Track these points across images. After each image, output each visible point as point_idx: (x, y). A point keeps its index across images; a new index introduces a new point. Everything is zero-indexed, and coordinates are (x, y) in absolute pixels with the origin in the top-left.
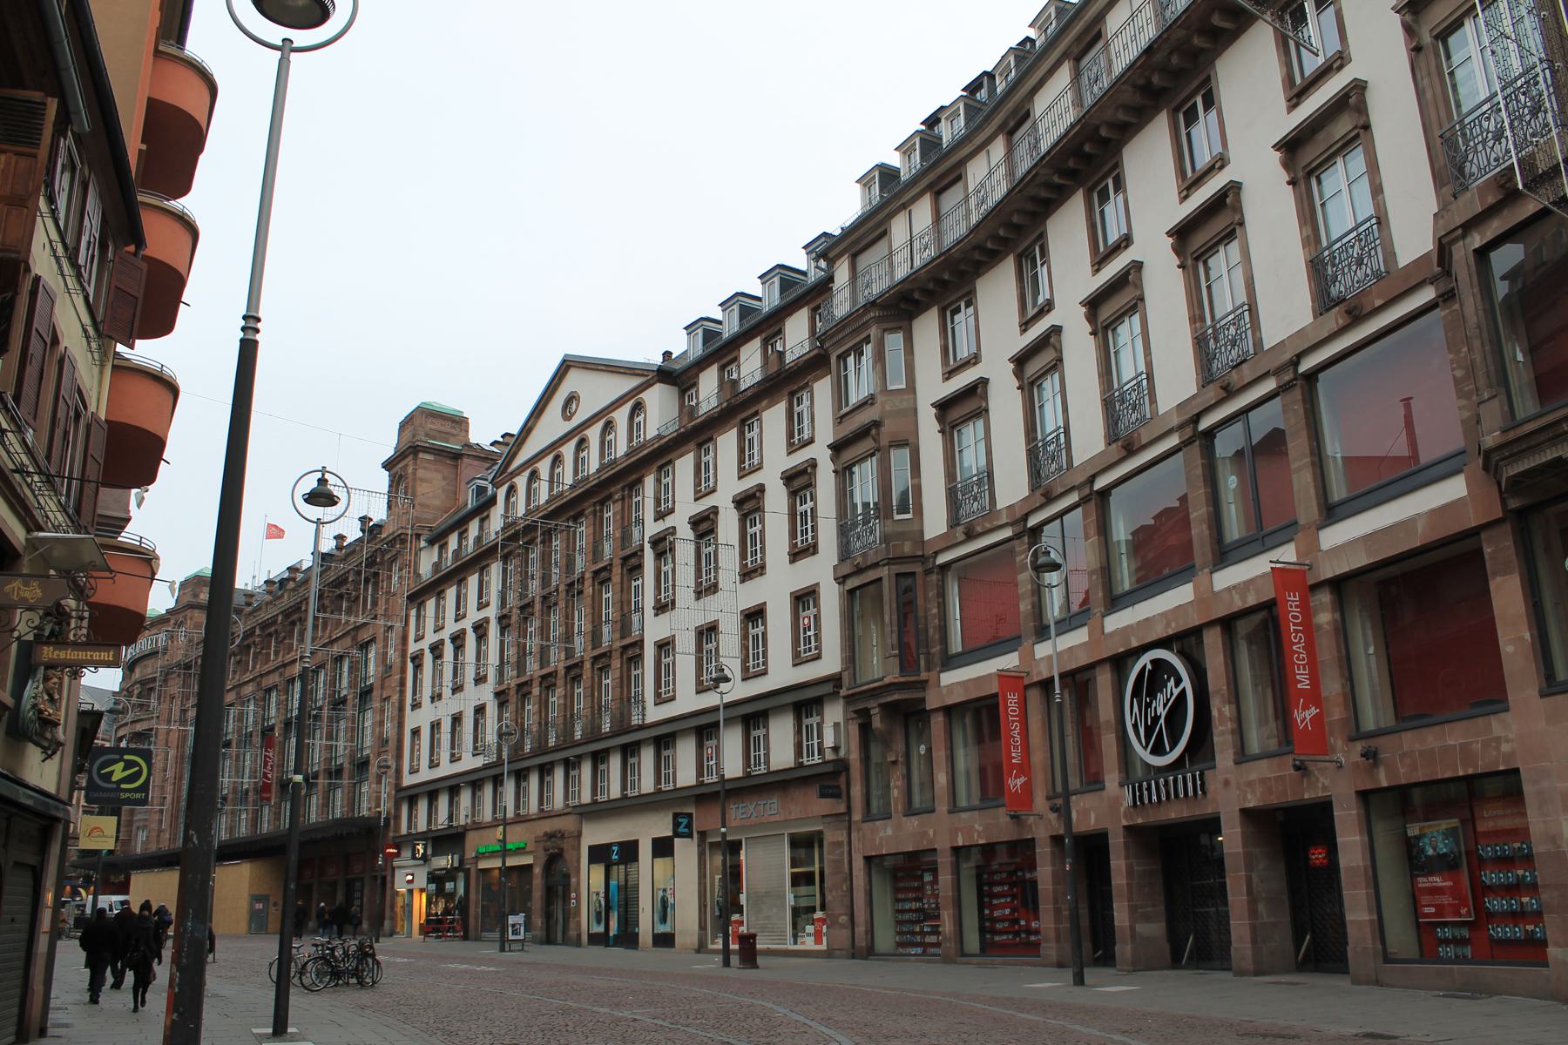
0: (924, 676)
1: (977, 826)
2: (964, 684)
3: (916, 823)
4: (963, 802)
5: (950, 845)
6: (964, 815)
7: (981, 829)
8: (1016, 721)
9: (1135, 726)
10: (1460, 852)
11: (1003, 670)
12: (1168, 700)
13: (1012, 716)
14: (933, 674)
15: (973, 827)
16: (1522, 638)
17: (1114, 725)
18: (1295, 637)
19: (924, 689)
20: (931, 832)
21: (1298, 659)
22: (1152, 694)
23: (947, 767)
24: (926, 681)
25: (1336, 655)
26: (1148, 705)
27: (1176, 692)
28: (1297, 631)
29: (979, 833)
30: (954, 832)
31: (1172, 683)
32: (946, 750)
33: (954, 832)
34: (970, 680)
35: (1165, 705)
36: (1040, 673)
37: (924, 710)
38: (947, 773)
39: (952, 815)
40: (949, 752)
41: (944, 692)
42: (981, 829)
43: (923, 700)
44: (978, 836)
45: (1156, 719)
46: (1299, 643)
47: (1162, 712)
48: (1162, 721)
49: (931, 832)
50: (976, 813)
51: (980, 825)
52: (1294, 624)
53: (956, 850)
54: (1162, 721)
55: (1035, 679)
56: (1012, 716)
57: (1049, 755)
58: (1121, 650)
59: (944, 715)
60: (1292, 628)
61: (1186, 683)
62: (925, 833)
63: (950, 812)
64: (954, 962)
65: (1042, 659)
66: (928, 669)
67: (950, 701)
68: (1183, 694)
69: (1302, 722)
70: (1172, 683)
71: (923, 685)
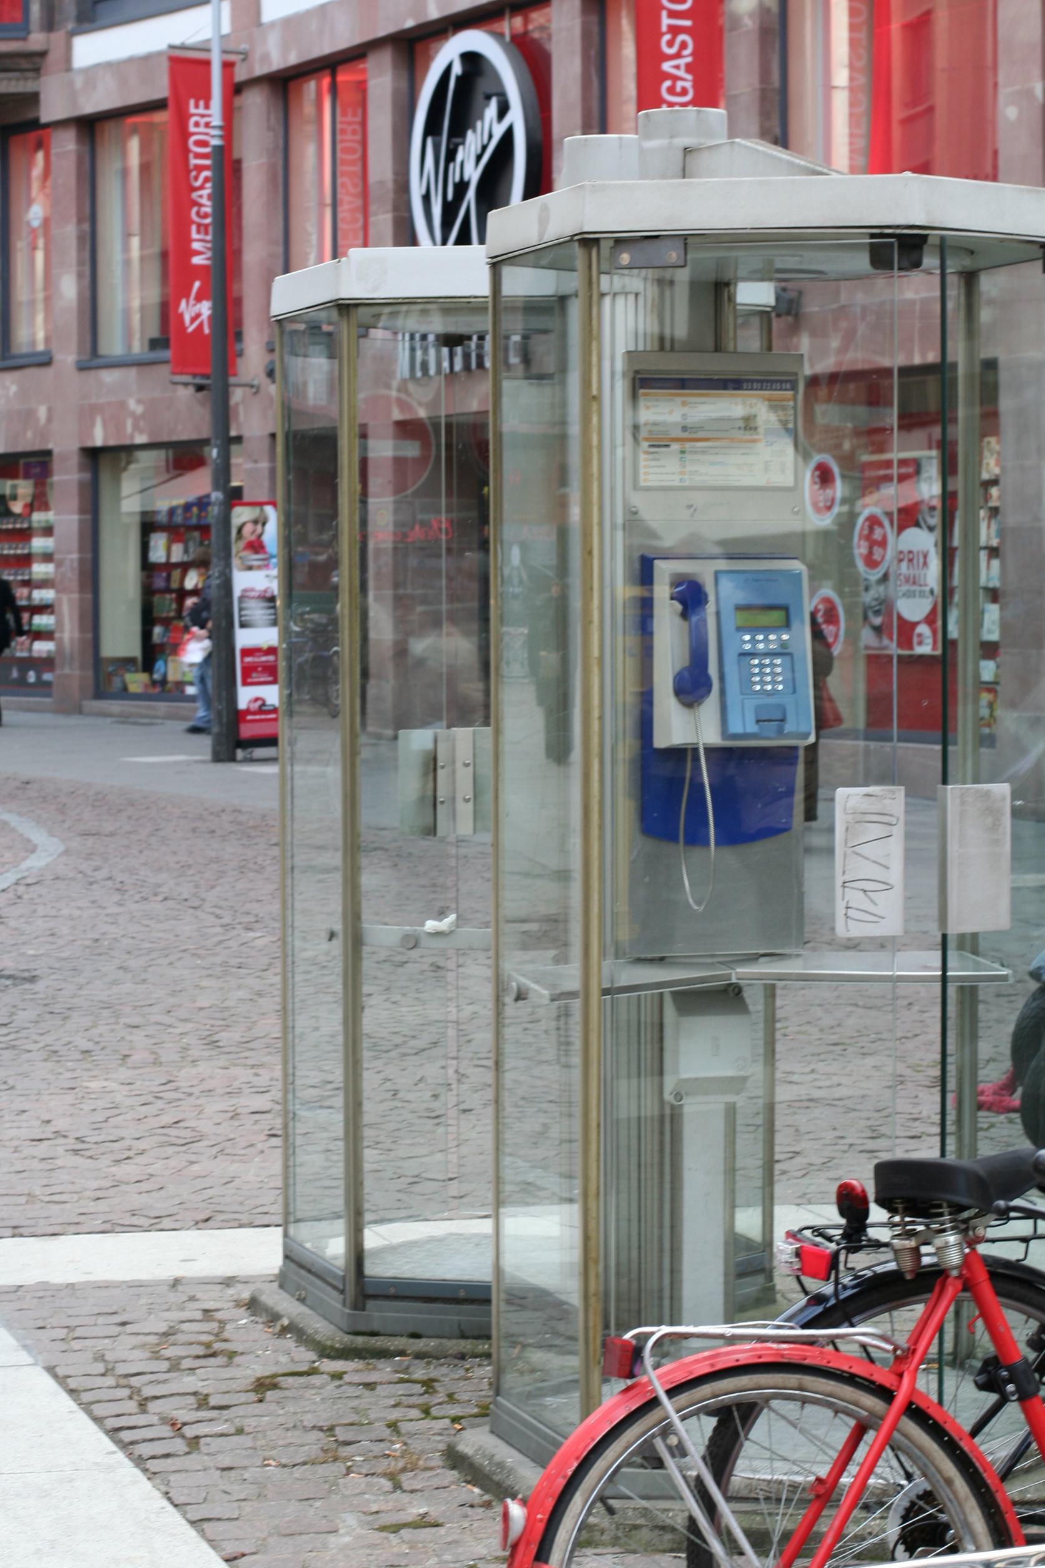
0: (36, 40)
1: (133, 405)
2: (115, 67)
3: (14, 389)
4: (113, 344)
5: (56, 451)
6: (109, 377)
7: (139, 409)
8: (205, 168)
9: (426, 199)
10: (440, 529)
11: (183, 47)
12: (484, 148)
13: (198, 156)
14: (58, 36)
15: (122, 405)
16: (1030, 93)
17: (391, 195)
18: (670, 44)
19: (37, 71)
20: (42, 412)
21: (671, 91)
22: (459, 130)
23: (80, 263)
24: (43, 54)
25: (757, 86)
26: (451, 156)
27: (499, 131)
28: (675, 31)
29: (136, 419)
30: (87, 414)
31: (491, 111)
32: (80, 221)
33: (87, 414)
34: (131, 60)
35: (479, 158)
36: (266, 58)
37: (35, 124)
38: (80, 276)
39: (85, 374)
40: (86, 227)
41: (79, 82)
42: (139, 409)
43: (33, 99)
44: (136, 427)
45: (462, 187)
46: (678, 55)
47: (474, 174)
48: (471, 194)
49: (42, 412)
50: (133, 372)
51: (139, 401)
52: (673, 14)
53: (93, 456)
54: (471, 194)
55: (259, 70)
56: (198, 156)
57: (280, 249)
58: (410, 23)
59: (80, 140)
60: (666, 21)
61: (516, 117)
62: (29, 415)
63: (82, 367)
64: (79, 711)
65: (273, 24)
66: (50, 25)
67: (90, 105)
68: (508, 137)
69: (193, 320)
70: (491, 111)
71: (34, 61)
